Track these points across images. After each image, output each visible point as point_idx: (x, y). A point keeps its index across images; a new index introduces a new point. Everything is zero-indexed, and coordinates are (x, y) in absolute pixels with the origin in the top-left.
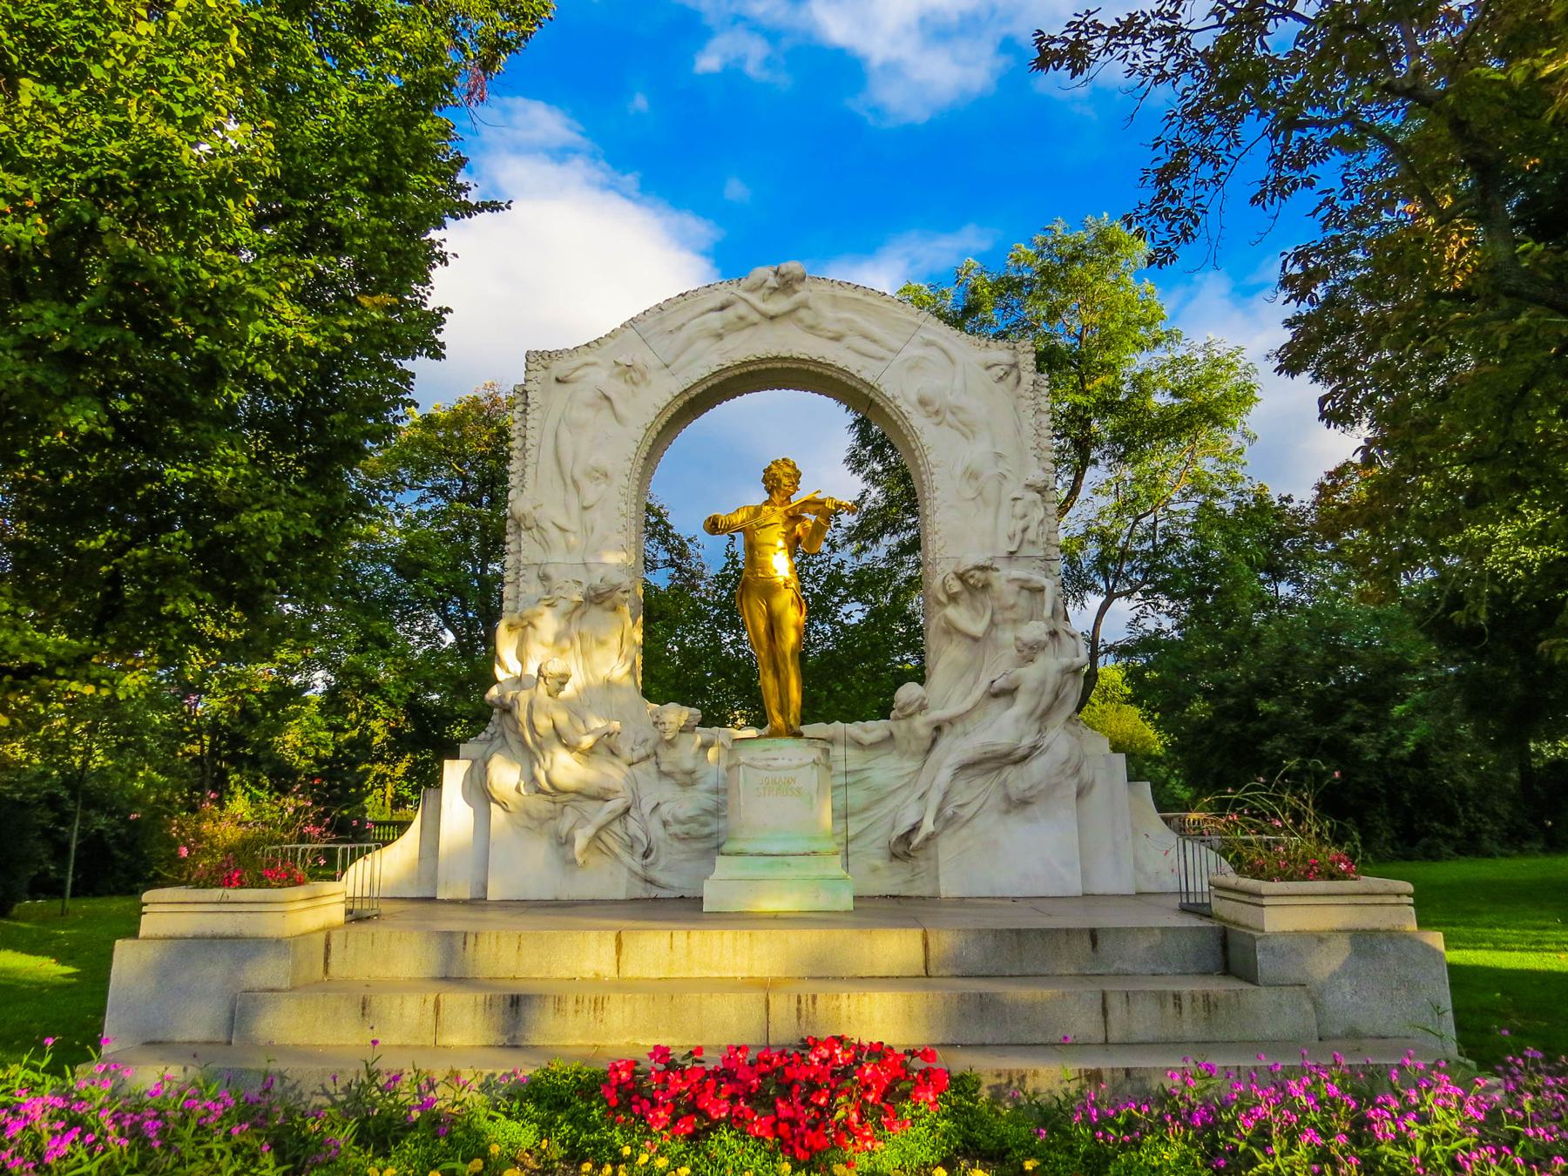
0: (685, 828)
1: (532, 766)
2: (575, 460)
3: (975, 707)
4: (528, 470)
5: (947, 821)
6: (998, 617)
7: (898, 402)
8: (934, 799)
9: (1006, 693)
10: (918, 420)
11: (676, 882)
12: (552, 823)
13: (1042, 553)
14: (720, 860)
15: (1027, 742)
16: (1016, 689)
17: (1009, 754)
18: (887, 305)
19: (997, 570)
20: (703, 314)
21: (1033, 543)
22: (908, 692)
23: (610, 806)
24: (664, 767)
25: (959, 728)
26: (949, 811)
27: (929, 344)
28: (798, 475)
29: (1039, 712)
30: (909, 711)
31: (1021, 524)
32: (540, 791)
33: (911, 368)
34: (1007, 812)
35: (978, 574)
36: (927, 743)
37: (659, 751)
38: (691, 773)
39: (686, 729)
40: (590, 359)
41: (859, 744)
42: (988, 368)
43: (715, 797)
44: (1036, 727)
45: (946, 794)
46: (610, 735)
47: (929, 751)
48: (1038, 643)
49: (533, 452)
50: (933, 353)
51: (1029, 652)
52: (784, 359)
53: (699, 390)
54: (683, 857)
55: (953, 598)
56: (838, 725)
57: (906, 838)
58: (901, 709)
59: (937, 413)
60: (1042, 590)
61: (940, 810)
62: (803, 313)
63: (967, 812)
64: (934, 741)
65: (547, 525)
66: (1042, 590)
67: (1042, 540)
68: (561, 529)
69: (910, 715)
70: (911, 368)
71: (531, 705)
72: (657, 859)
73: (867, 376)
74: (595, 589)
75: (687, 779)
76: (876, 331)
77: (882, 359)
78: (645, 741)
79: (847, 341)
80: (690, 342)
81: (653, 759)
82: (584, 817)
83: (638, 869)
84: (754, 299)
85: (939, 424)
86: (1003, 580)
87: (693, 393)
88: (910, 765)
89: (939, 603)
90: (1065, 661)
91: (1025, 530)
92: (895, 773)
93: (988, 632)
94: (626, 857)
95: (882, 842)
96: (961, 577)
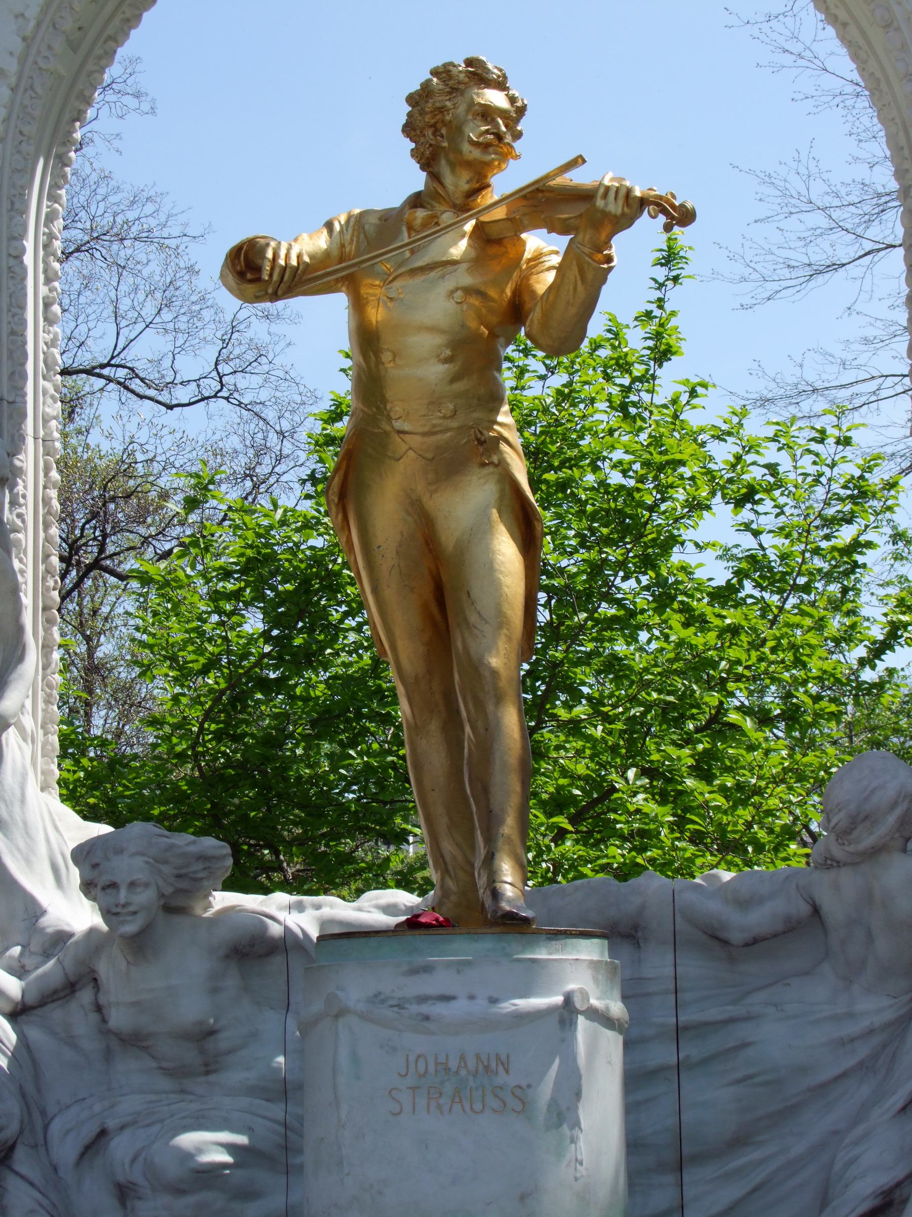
24: (118, 1019)
30: (868, 841)
37: (103, 969)
43: (277, 1111)
75: (190, 1055)
78: (61, 937)
81: (85, 996)
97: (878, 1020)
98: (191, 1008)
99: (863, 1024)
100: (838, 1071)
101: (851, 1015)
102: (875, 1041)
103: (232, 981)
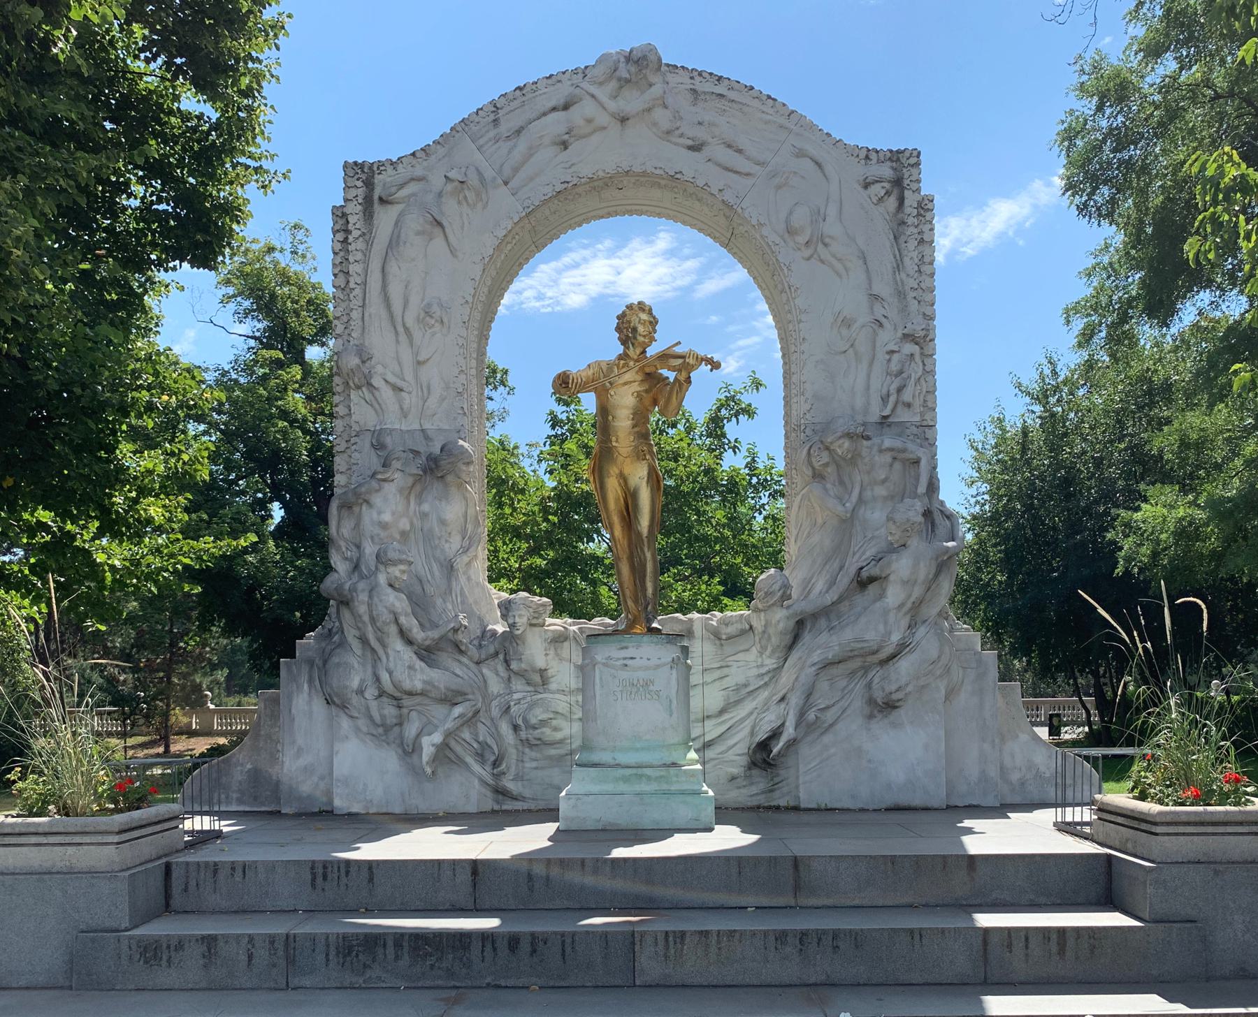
3: (841, 599)
5: (809, 726)
8: (795, 700)
18: (756, 103)
28: (654, 322)
45: (809, 696)
57: (764, 746)
61: (802, 714)
76: (742, 142)
77: (748, 174)
79: (706, 151)
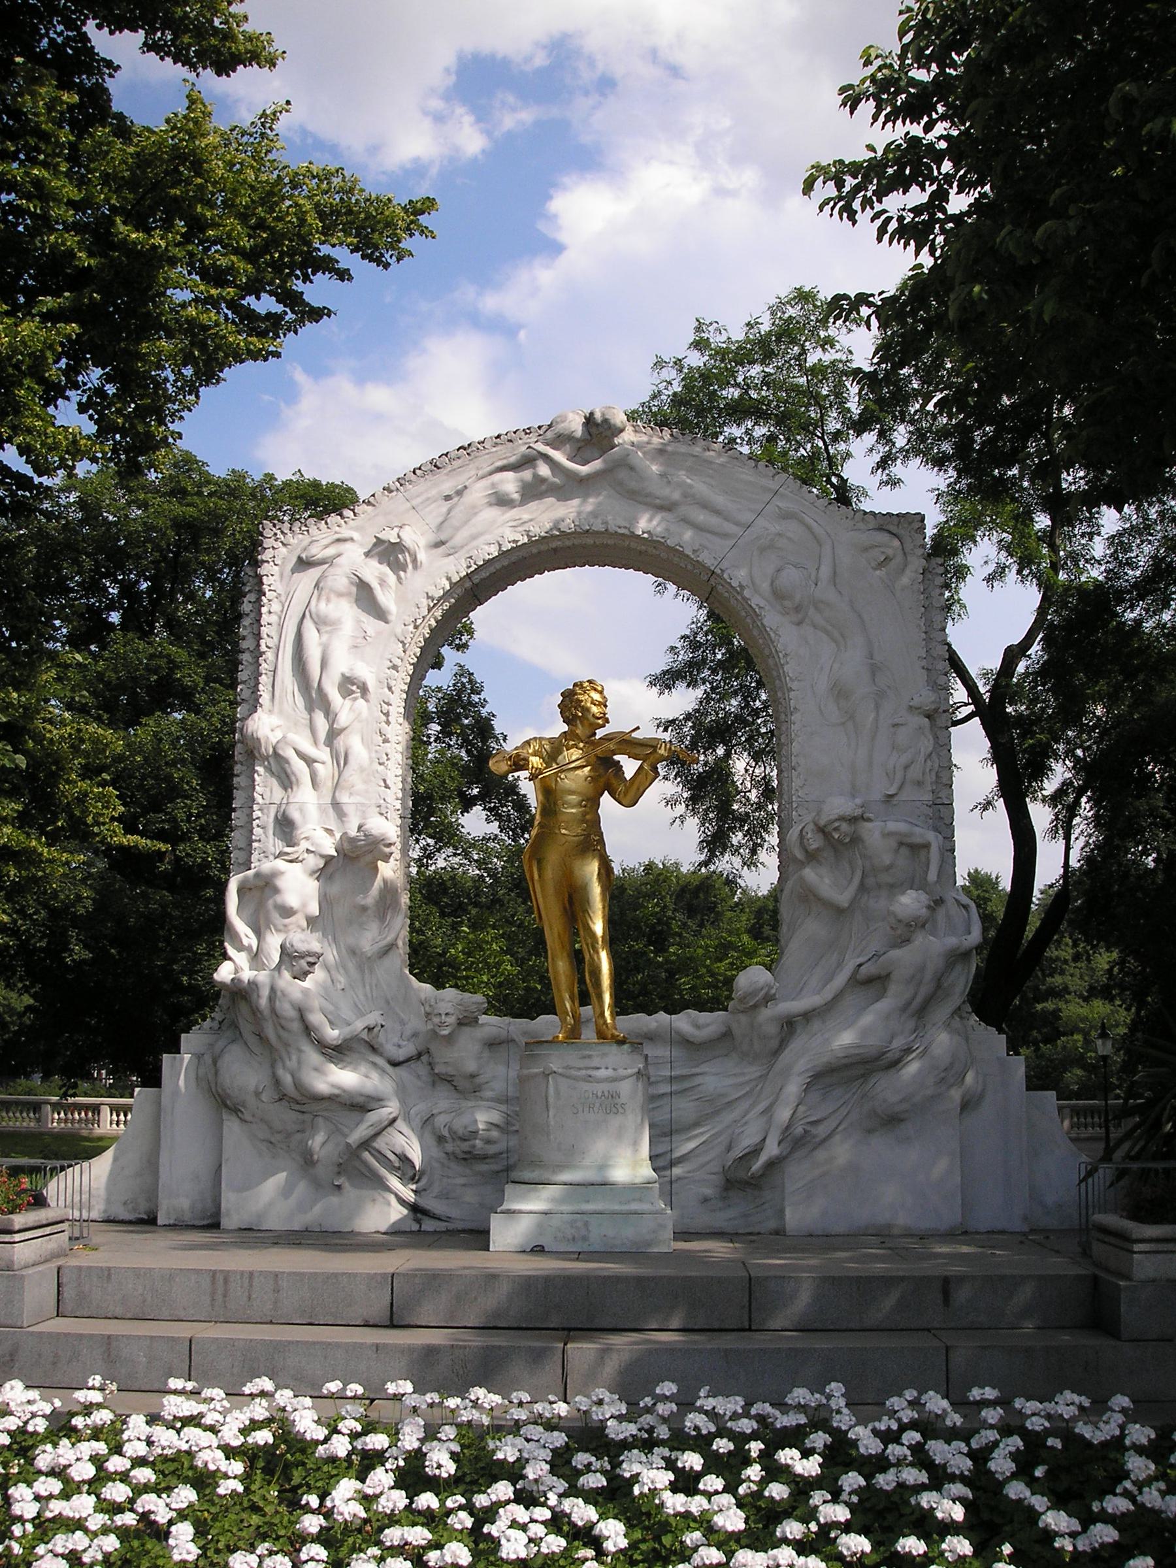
0: (465, 1146)
1: (273, 1066)
2: (324, 664)
4: (263, 679)
6: (870, 881)
7: (747, 593)
9: (871, 983)
10: (771, 619)
11: (454, 1213)
12: (298, 1136)
13: (928, 797)
14: (509, 1188)
15: (898, 1043)
16: (888, 975)
17: (877, 1059)
19: (869, 820)
20: (491, 473)
21: (919, 784)
22: (753, 977)
23: (372, 1117)
25: (816, 1025)
26: (799, 1130)
27: (786, 516)
29: (915, 1005)
31: (905, 759)
32: (283, 1097)
33: (763, 550)
34: (870, 1131)
35: (844, 826)
36: (774, 1044)
37: (433, 1049)
38: (472, 1076)
39: (467, 1021)
40: (345, 533)
41: (686, 1043)
42: (866, 549)
43: (503, 1107)
44: (911, 1024)
46: (370, 1029)
47: (777, 1052)
48: (916, 919)
49: (270, 655)
50: (792, 529)
51: (906, 931)
52: (597, 533)
53: (484, 574)
54: (462, 1181)
55: (812, 857)
56: (662, 1016)
58: (742, 1000)
59: (798, 609)
60: (927, 846)
62: (622, 474)
63: (821, 1131)
64: (783, 1043)
65: (290, 754)
66: (927, 846)
67: (930, 779)
68: (309, 761)
69: (755, 1007)
70: (763, 550)
71: (273, 990)
72: (430, 1183)
73: (707, 559)
74: (353, 840)
77: (725, 536)
80: (474, 511)
81: (424, 1058)
82: (338, 1130)
83: (410, 1197)
84: (558, 456)
85: (799, 624)
86: (877, 835)
87: (476, 579)
88: (753, 1071)
89: (795, 860)
90: (952, 941)
91: (906, 767)
92: (731, 1081)
93: (853, 902)
94: (394, 1182)
95: (715, 1167)
96: (822, 830)
97: (753, 1076)
98: (471, 1066)
99: (747, 1078)
100: (737, 1096)
101: (743, 1074)
102: (754, 1083)
103: (486, 1054)
